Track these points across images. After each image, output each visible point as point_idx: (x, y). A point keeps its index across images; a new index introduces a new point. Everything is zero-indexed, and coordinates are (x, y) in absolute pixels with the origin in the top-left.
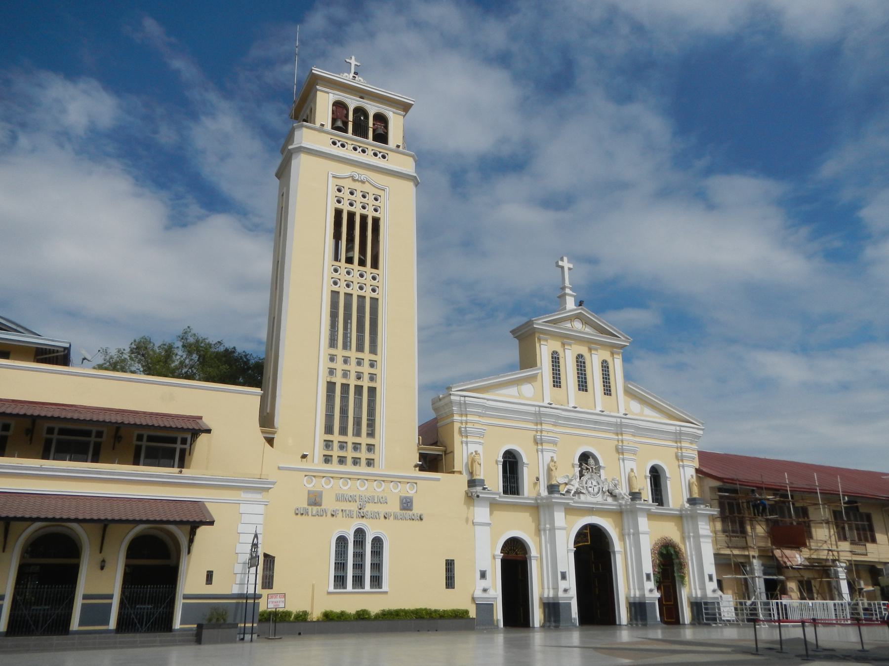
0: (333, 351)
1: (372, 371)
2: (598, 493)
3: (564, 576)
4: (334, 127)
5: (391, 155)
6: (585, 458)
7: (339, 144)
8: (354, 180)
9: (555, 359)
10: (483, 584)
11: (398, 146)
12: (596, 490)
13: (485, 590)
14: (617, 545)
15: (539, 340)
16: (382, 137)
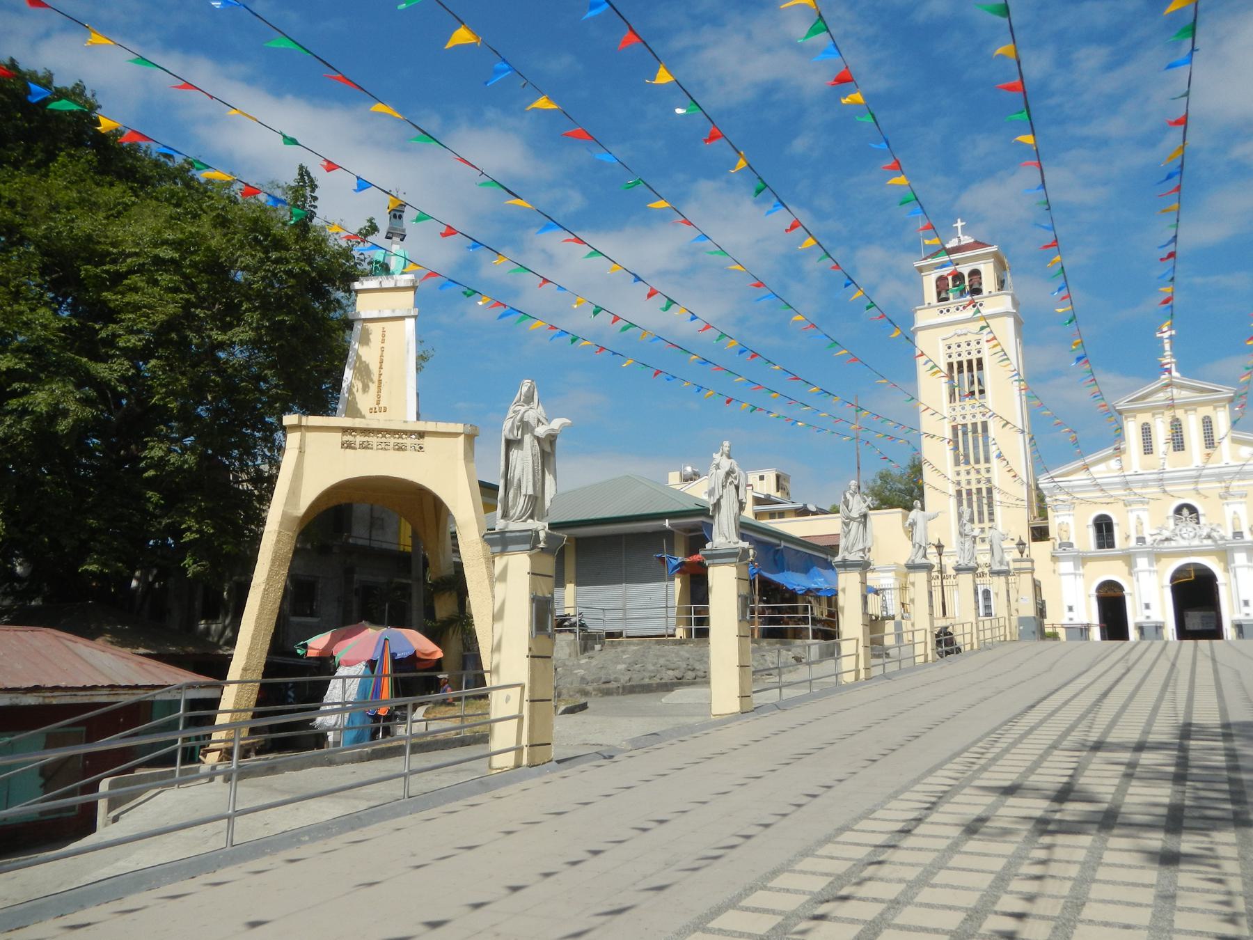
0: (958, 468)
1: (987, 475)
2: (1194, 537)
3: (1147, 606)
4: (940, 300)
5: (986, 302)
6: (1178, 510)
7: (945, 311)
8: (959, 336)
9: (1146, 431)
10: (1071, 615)
11: (990, 292)
12: (1192, 534)
13: (1071, 619)
14: (1221, 578)
15: (1126, 418)
16: (977, 291)
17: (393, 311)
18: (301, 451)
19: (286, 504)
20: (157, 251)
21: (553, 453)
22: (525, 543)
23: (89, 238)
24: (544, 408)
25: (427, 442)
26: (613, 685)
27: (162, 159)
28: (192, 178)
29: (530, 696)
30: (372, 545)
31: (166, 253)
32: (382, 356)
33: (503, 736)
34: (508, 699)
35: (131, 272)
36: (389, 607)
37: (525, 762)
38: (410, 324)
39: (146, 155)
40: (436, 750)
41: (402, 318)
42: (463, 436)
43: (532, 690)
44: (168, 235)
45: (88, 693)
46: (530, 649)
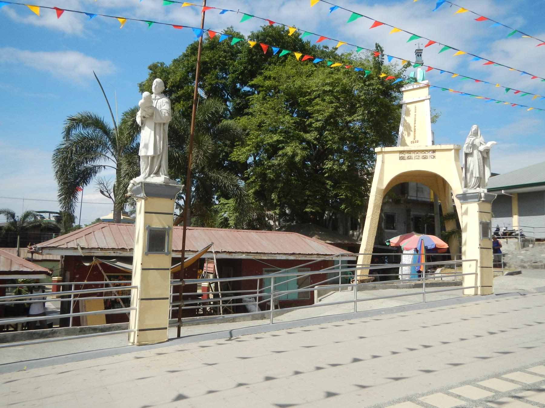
17: (419, 98)
18: (383, 162)
19: (378, 184)
20: (324, 88)
21: (488, 157)
22: (475, 198)
23: (300, 87)
24: (483, 137)
25: (437, 154)
26: (539, 264)
27: (324, 49)
28: (336, 55)
29: (480, 265)
30: (418, 199)
31: (327, 88)
32: (415, 118)
33: (469, 281)
34: (470, 266)
35: (315, 98)
36: (427, 226)
37: (479, 293)
38: (428, 102)
39: (318, 49)
40: (443, 286)
41: (424, 100)
42: (453, 150)
43: (481, 262)
44: (328, 81)
45: (310, 256)
46: (480, 245)
